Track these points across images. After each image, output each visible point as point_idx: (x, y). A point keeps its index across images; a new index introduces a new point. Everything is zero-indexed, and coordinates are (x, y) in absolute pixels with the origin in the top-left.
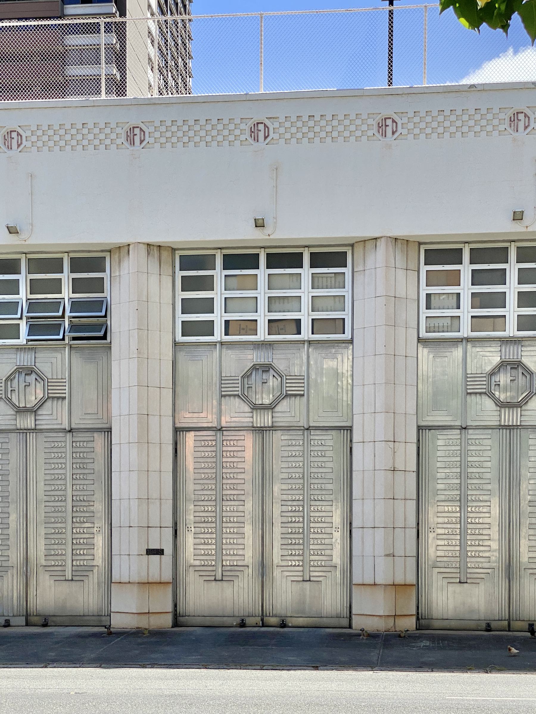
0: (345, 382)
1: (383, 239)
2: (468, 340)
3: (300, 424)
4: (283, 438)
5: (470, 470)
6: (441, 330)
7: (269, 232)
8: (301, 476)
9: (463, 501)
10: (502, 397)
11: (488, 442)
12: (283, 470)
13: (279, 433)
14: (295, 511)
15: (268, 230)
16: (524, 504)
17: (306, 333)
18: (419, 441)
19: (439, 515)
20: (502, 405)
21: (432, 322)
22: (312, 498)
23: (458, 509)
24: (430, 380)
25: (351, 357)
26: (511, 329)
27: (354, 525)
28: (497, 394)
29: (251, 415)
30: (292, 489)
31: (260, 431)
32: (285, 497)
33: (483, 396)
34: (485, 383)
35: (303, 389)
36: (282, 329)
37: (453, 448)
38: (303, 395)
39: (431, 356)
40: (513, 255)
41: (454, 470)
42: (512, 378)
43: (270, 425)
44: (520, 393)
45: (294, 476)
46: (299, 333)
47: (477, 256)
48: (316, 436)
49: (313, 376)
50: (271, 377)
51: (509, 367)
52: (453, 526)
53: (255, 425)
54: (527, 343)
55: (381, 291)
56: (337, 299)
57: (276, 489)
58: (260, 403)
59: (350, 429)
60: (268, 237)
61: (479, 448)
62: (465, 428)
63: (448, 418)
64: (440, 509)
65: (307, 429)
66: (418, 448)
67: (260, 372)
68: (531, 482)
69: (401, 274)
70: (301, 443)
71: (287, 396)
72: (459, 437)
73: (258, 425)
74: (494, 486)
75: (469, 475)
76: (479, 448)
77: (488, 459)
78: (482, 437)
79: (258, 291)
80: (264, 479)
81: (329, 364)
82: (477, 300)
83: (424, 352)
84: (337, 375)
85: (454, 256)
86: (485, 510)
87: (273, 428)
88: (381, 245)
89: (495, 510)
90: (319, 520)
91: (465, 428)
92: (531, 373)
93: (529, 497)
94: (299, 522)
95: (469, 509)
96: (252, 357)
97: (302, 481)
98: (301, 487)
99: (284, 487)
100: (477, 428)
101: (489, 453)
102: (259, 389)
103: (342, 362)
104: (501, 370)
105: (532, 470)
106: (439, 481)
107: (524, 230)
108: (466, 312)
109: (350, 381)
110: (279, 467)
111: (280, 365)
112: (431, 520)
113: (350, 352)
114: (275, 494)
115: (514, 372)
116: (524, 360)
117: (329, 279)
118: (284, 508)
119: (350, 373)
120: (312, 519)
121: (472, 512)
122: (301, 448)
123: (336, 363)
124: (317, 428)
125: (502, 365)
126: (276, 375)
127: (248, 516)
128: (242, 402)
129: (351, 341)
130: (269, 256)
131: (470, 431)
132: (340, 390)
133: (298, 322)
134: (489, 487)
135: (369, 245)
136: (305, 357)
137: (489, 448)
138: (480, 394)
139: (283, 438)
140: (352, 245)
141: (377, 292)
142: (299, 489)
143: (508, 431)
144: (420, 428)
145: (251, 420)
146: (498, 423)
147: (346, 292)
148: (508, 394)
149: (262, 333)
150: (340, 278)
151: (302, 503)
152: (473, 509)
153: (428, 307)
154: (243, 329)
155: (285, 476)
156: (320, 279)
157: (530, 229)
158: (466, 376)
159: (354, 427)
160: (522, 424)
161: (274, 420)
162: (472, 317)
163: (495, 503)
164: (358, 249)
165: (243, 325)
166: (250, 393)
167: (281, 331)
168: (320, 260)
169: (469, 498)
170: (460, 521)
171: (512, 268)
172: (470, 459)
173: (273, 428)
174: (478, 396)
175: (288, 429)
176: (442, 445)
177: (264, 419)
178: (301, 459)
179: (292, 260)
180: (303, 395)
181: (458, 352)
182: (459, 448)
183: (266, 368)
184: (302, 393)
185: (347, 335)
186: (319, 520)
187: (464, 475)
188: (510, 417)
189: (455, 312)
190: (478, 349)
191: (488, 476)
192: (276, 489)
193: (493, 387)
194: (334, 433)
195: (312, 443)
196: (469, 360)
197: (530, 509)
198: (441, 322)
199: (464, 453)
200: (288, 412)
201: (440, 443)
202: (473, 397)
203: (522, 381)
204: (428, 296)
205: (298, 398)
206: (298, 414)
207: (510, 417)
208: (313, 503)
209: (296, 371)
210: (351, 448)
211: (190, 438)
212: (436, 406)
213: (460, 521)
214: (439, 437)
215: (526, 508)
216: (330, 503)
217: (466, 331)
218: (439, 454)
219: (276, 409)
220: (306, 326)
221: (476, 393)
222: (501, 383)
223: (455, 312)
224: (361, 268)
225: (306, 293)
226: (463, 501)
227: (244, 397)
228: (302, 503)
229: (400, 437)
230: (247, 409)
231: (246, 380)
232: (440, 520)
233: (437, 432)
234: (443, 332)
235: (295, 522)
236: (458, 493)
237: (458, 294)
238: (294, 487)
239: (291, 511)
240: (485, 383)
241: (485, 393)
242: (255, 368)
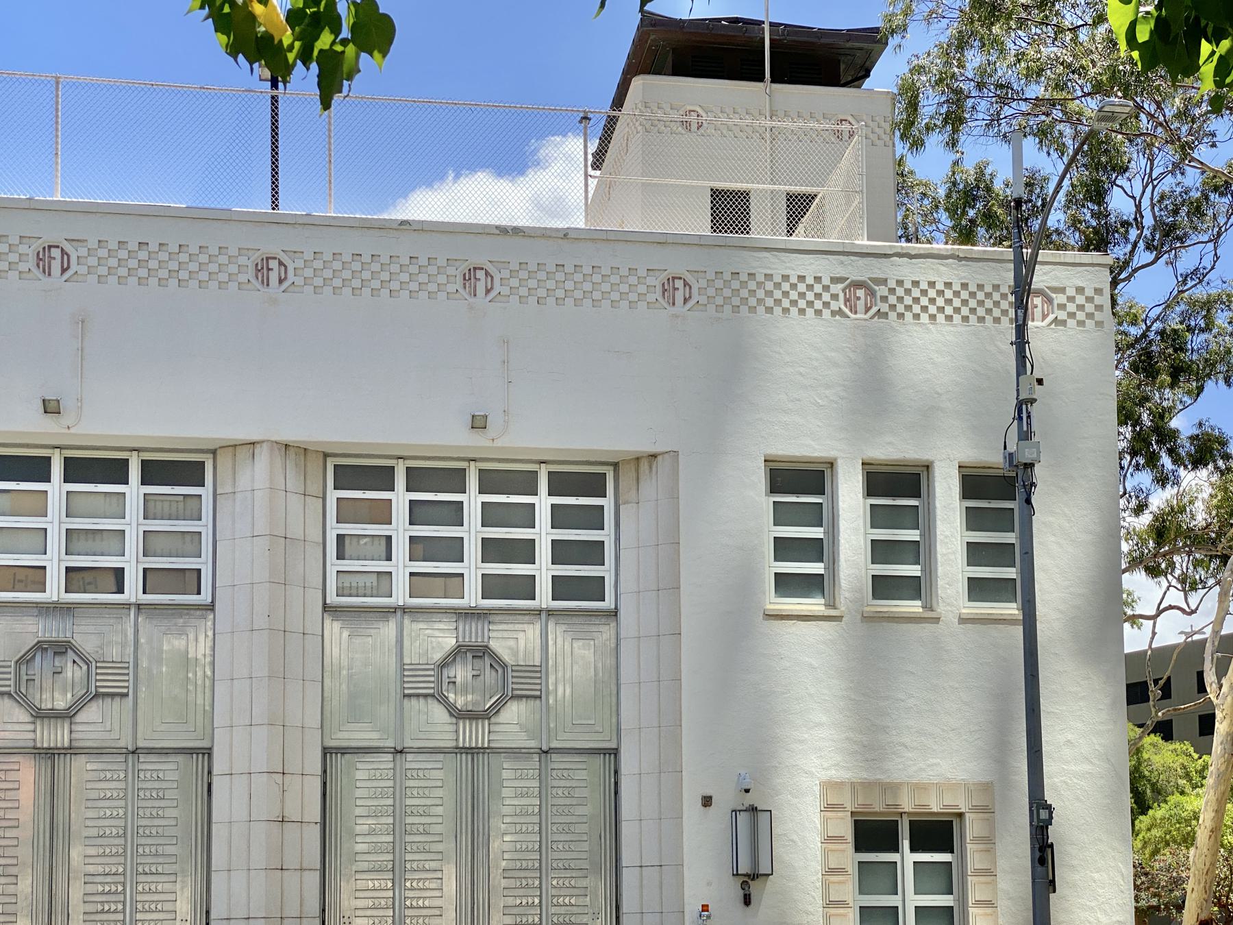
0: (200, 674)
1: (265, 445)
2: (405, 610)
3: (122, 744)
4: (89, 767)
5: (409, 820)
6: (361, 591)
7: (69, 423)
8: (121, 832)
9: (397, 872)
10: (460, 702)
11: (438, 774)
12: (88, 823)
13: (83, 758)
14: (109, 893)
15: (67, 419)
16: (496, 875)
17: (133, 589)
18: (325, 772)
19: (359, 894)
20: (459, 715)
21: (347, 580)
22: (140, 870)
23: (390, 884)
24: (344, 672)
25: (210, 633)
26: (472, 596)
27: (213, 916)
28: (451, 696)
29: (31, 727)
30: (104, 855)
32: (91, 869)
33: (430, 700)
34: (432, 679)
35: (126, 684)
36: (89, 583)
37: (383, 784)
38: (126, 695)
39: (345, 634)
40: (473, 482)
41: (384, 820)
42: (475, 673)
43: (66, 745)
44: (487, 696)
45: (108, 832)
46: (121, 590)
47: (416, 479)
48: (148, 764)
49: (144, 663)
50: (70, 664)
51: (469, 656)
52: (381, 913)
53: (39, 745)
54: (498, 618)
55: (261, 527)
56: (188, 537)
57: (76, 854)
58: (49, 706)
59: (208, 752)
60: (66, 431)
61: (422, 783)
62: (401, 752)
63: (375, 735)
64: (360, 885)
65: (133, 753)
66: (325, 783)
67: (50, 653)
68: (507, 838)
70: (122, 776)
71: (97, 695)
72: (391, 765)
73: (45, 745)
74: (448, 846)
75: (408, 827)
76: (422, 783)
77: (439, 802)
78: (429, 766)
79: (49, 518)
80: (54, 835)
81: (173, 644)
82: (419, 548)
83: (334, 629)
84: (186, 662)
85: (382, 477)
86: (433, 886)
88: (263, 455)
89: (450, 886)
90: (153, 906)
91: (401, 752)
92: (504, 666)
93: (504, 864)
94: (115, 912)
95: (408, 884)
96: (35, 629)
97: (122, 841)
98: (121, 851)
99: (92, 851)
100: (421, 751)
101: (439, 793)
102: (47, 683)
103: (197, 642)
104: (458, 659)
105: (507, 820)
106: (359, 839)
108: (401, 566)
109: (209, 673)
110: (80, 815)
112: (345, 904)
113: (210, 623)
114: (74, 863)
115: (478, 662)
116: (493, 644)
117: (174, 505)
118: (90, 888)
119: (208, 659)
120: (139, 906)
121: (412, 889)
122: (122, 785)
123: (184, 643)
124: (151, 751)
125: (459, 652)
126: (77, 659)
127: (22, 903)
128: (15, 704)
129: (211, 607)
130: (68, 461)
131: (410, 757)
132: (191, 687)
133: (119, 573)
134: (440, 847)
135: (243, 453)
136: (130, 632)
137: (439, 784)
138: (426, 696)
139: (89, 767)
140: (214, 452)
141: (251, 527)
142: (117, 855)
143: (470, 756)
144: (326, 751)
145: (31, 736)
146: (453, 744)
147: (203, 526)
148: (470, 697)
149: (54, 589)
150: (192, 503)
151: (121, 879)
152: (414, 884)
154: (20, 581)
155: (94, 832)
156: (159, 505)
158: (402, 666)
159: (215, 749)
160: (492, 745)
161: (74, 735)
162: (411, 574)
163: (450, 873)
164: (224, 459)
165: (21, 575)
166: (31, 691)
167: (88, 587)
168: (154, 472)
169: (408, 866)
170: (394, 904)
171: (473, 501)
172: (409, 802)
174: (422, 700)
176: (365, 780)
177: (58, 736)
178: (122, 803)
179: (115, 471)
180: (126, 695)
181: (389, 630)
182: (391, 783)
183: (61, 648)
184: (125, 691)
185: (205, 597)
186: (153, 906)
187: (399, 830)
188: (473, 734)
189: (383, 566)
190: (422, 626)
191: (438, 829)
192: (74, 854)
193: (444, 688)
194: (180, 758)
195: (142, 775)
196: (406, 643)
197: (504, 883)
198: (361, 580)
199: (399, 792)
200: (96, 723)
201: (360, 775)
202: (414, 701)
203: (489, 676)
205: (117, 699)
206: (117, 728)
207: (473, 734)
208: (141, 878)
209: (114, 653)
210: (210, 785)
212: (355, 714)
213: (394, 904)
214: (359, 766)
215: (498, 881)
216: (172, 878)
217: (401, 594)
218: (358, 793)
219: (78, 718)
220: (133, 581)
221: (418, 696)
222: (458, 680)
223: (383, 566)
224: (229, 489)
225: (134, 525)
226: (397, 872)
227: (18, 697)
228: (121, 879)
230: (28, 718)
231: (24, 668)
232: (360, 903)
233: (356, 758)
234: (365, 596)
235: (108, 911)
236: (390, 857)
237: (389, 538)
238: (108, 851)
239: (103, 893)
240: (432, 679)
241: (433, 696)
242: (40, 647)
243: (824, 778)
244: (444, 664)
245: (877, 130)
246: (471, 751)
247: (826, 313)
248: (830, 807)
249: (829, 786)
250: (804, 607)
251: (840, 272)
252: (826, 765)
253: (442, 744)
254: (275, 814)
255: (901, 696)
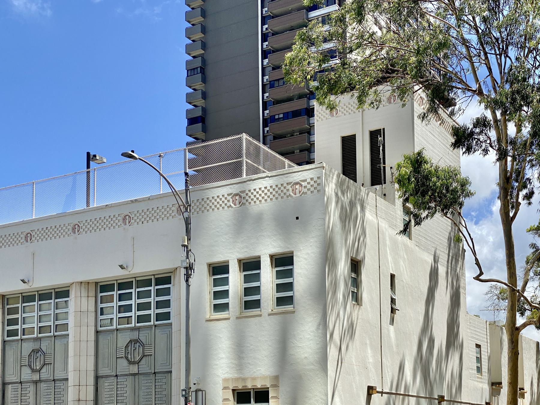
31: (36, 382)
63: (109, 371)
69: (84, 300)
87: (40, 381)
100: (122, 375)
107: (128, 273)
111: (44, 349)
153: (102, 314)
157: (131, 272)
173: (40, 381)
175: (46, 381)
204: (102, 309)
207: (134, 369)
211: (9, 388)
229: (83, 382)
243: (223, 378)
244: (127, 347)
245: (323, 113)
246: (134, 375)
247: (226, 208)
248: (225, 388)
249: (225, 380)
250: (222, 316)
251: (230, 191)
252: (224, 373)
253: (127, 373)
254: (77, 398)
255: (248, 345)
